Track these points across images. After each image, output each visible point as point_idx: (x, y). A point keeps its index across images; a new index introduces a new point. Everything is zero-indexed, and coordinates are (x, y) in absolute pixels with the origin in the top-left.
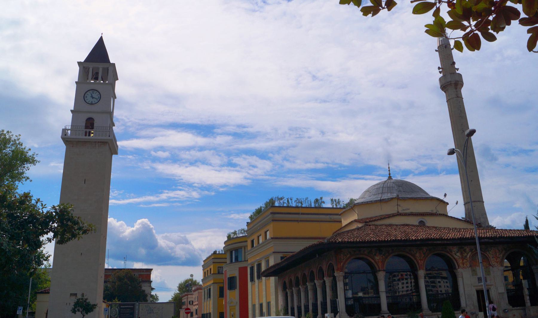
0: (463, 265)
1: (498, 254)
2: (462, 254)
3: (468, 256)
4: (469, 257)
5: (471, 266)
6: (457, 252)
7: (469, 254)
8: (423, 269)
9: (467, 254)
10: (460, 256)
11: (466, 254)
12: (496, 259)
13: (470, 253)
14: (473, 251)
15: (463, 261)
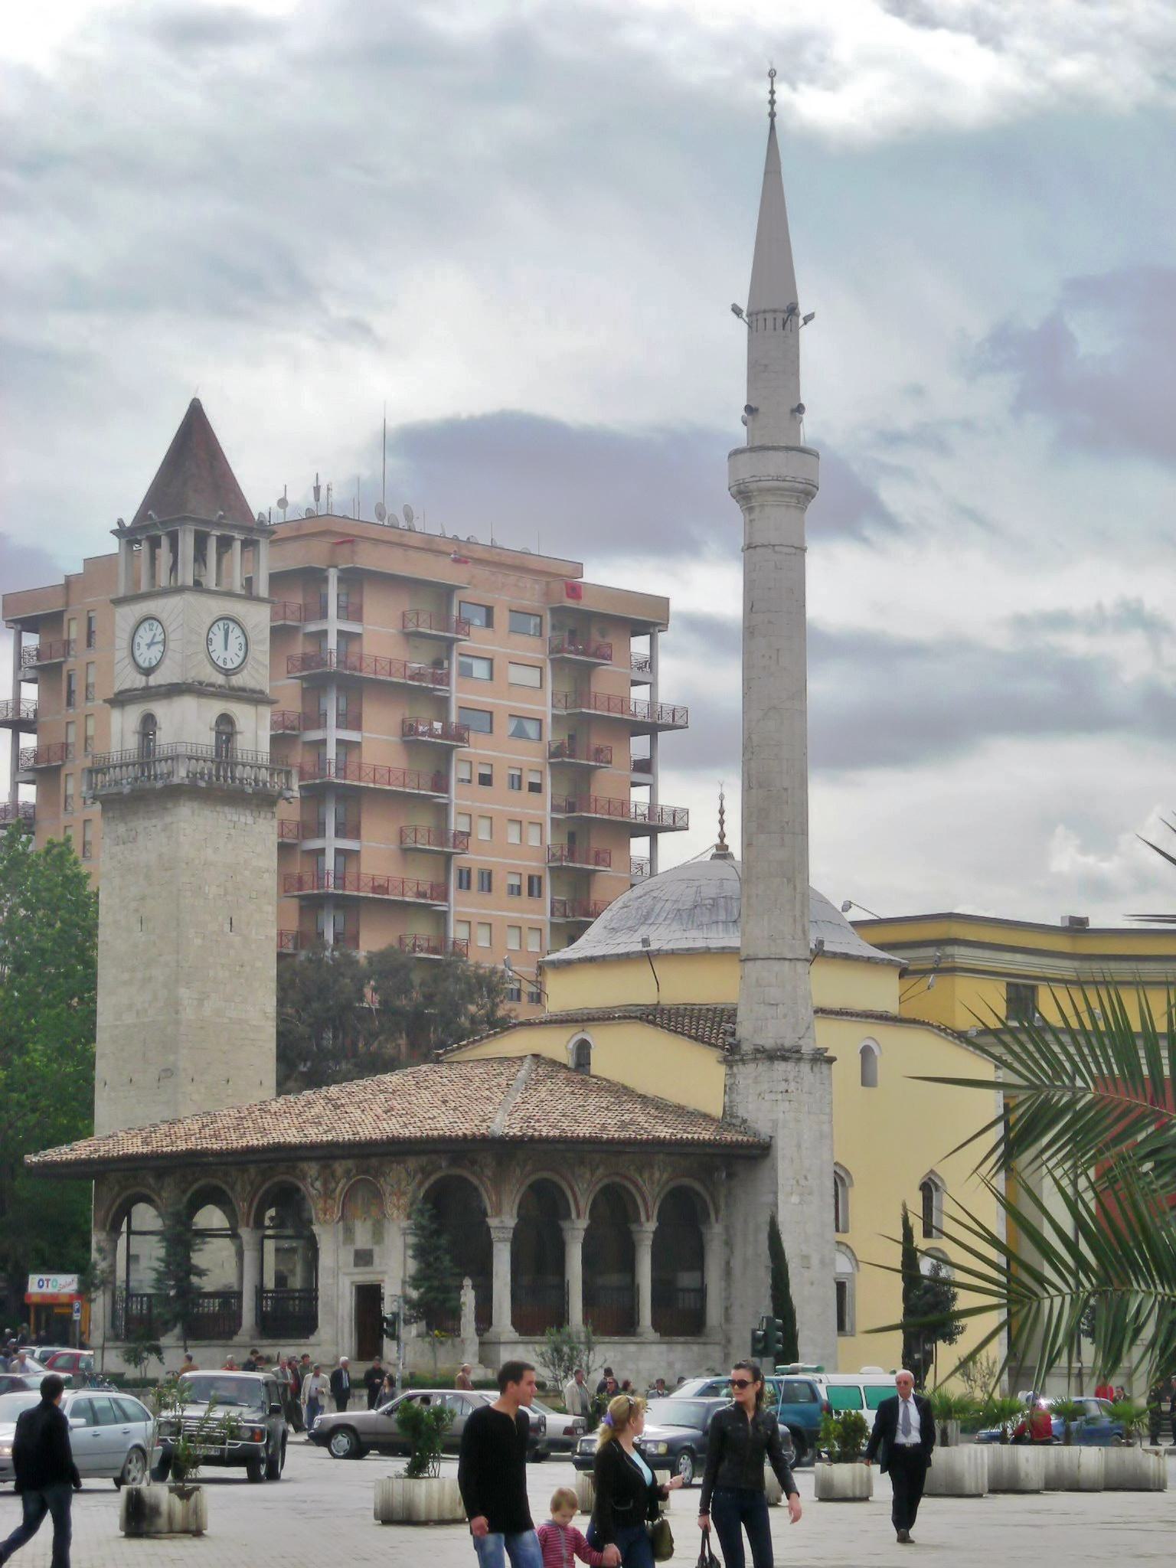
0: (325, 1214)
1: (403, 1184)
2: (325, 1184)
3: (338, 1190)
4: (340, 1195)
5: (342, 1218)
6: (317, 1179)
7: (341, 1185)
8: (248, 1225)
9: (337, 1183)
10: (321, 1190)
11: (333, 1185)
12: (398, 1200)
13: (343, 1181)
14: (352, 1174)
15: (325, 1202)
